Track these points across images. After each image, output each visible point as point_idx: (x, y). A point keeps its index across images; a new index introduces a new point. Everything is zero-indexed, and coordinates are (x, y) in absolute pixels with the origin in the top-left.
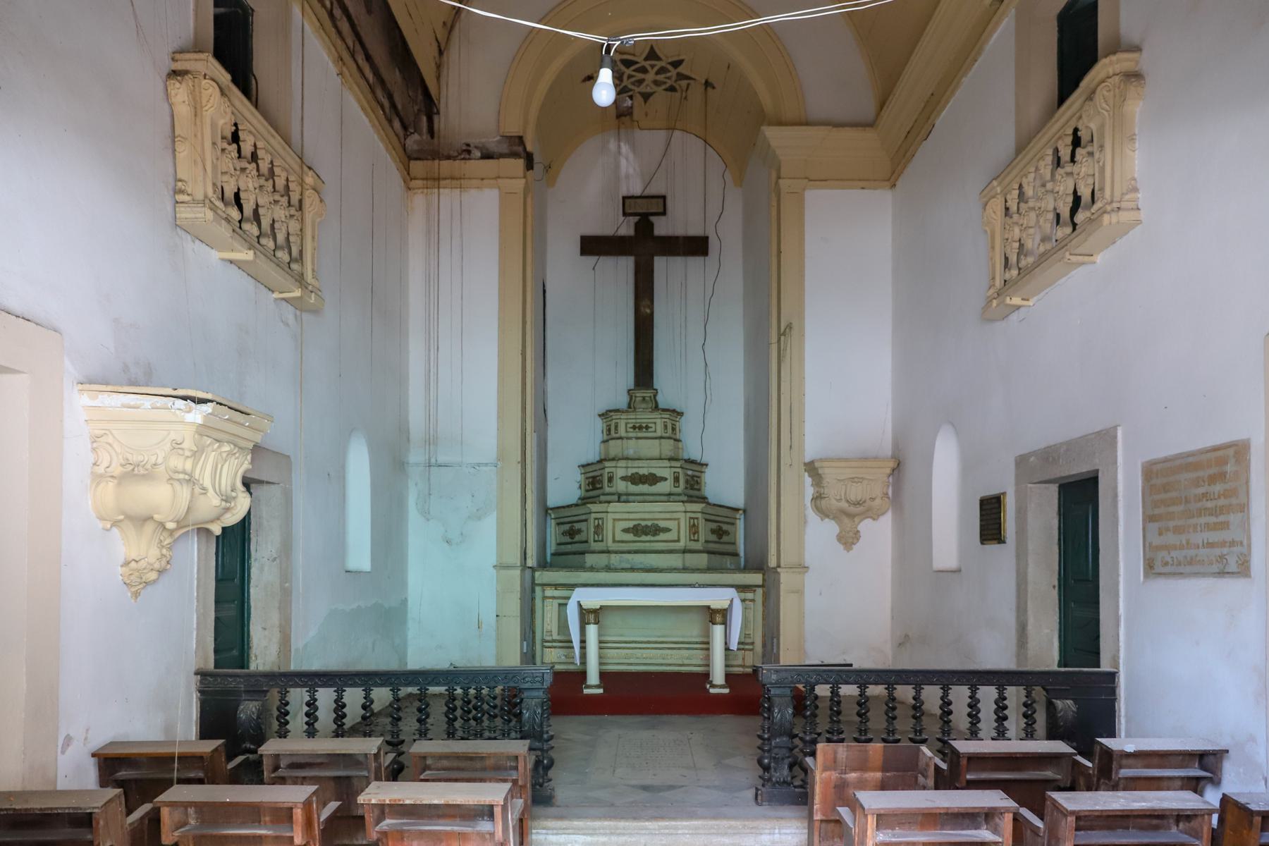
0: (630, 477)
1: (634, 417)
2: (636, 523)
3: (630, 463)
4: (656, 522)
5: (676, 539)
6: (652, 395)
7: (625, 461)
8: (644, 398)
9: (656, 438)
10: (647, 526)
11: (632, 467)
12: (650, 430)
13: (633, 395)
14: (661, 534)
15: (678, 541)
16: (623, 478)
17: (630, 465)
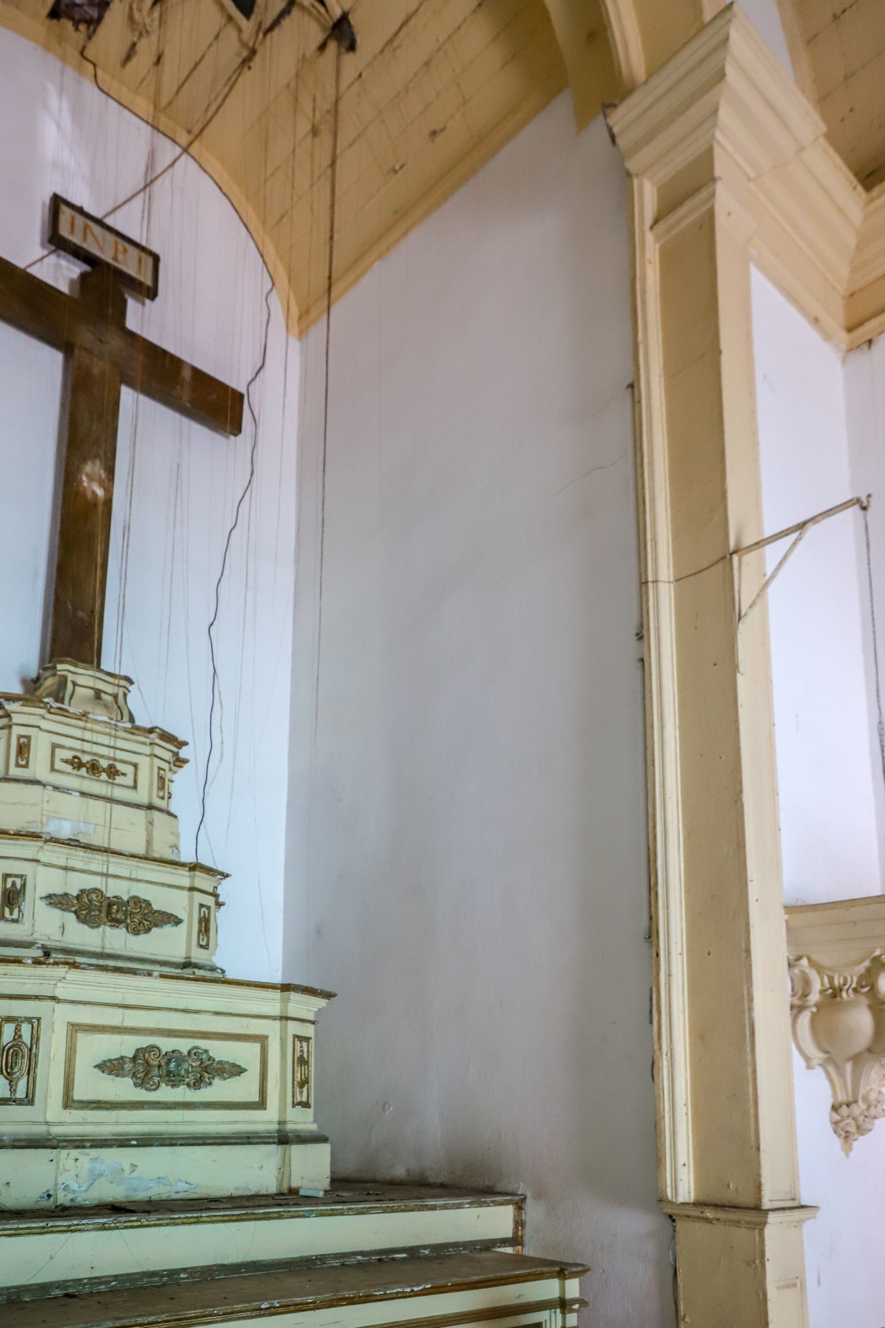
0: (78, 897)
1: (78, 733)
2: (144, 1041)
3: (78, 859)
4: (203, 1044)
5: (257, 1099)
6: (121, 691)
7: (65, 850)
8: (98, 694)
9: (138, 806)
10: (174, 1056)
11: (83, 871)
12: (119, 780)
13: (70, 677)
14: (217, 1081)
15: (261, 1104)
16: (57, 901)
17: (79, 865)
